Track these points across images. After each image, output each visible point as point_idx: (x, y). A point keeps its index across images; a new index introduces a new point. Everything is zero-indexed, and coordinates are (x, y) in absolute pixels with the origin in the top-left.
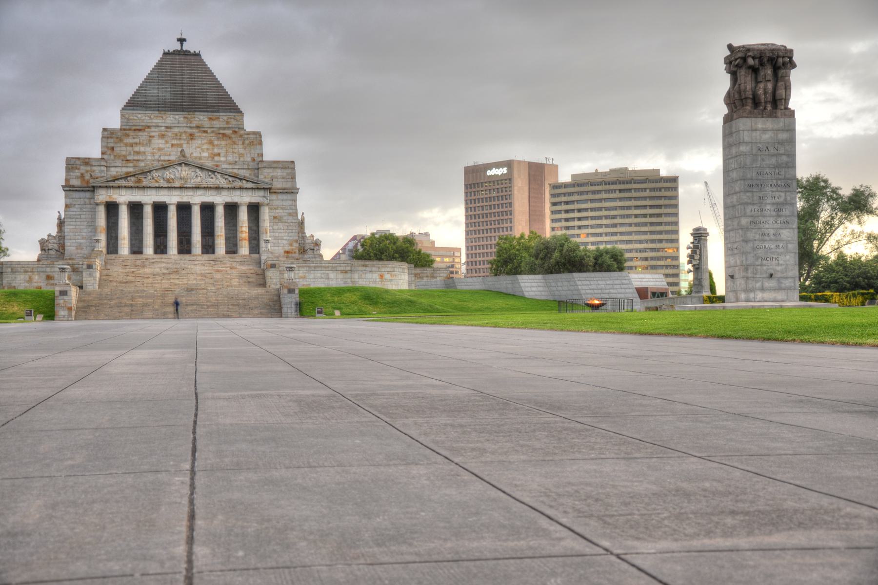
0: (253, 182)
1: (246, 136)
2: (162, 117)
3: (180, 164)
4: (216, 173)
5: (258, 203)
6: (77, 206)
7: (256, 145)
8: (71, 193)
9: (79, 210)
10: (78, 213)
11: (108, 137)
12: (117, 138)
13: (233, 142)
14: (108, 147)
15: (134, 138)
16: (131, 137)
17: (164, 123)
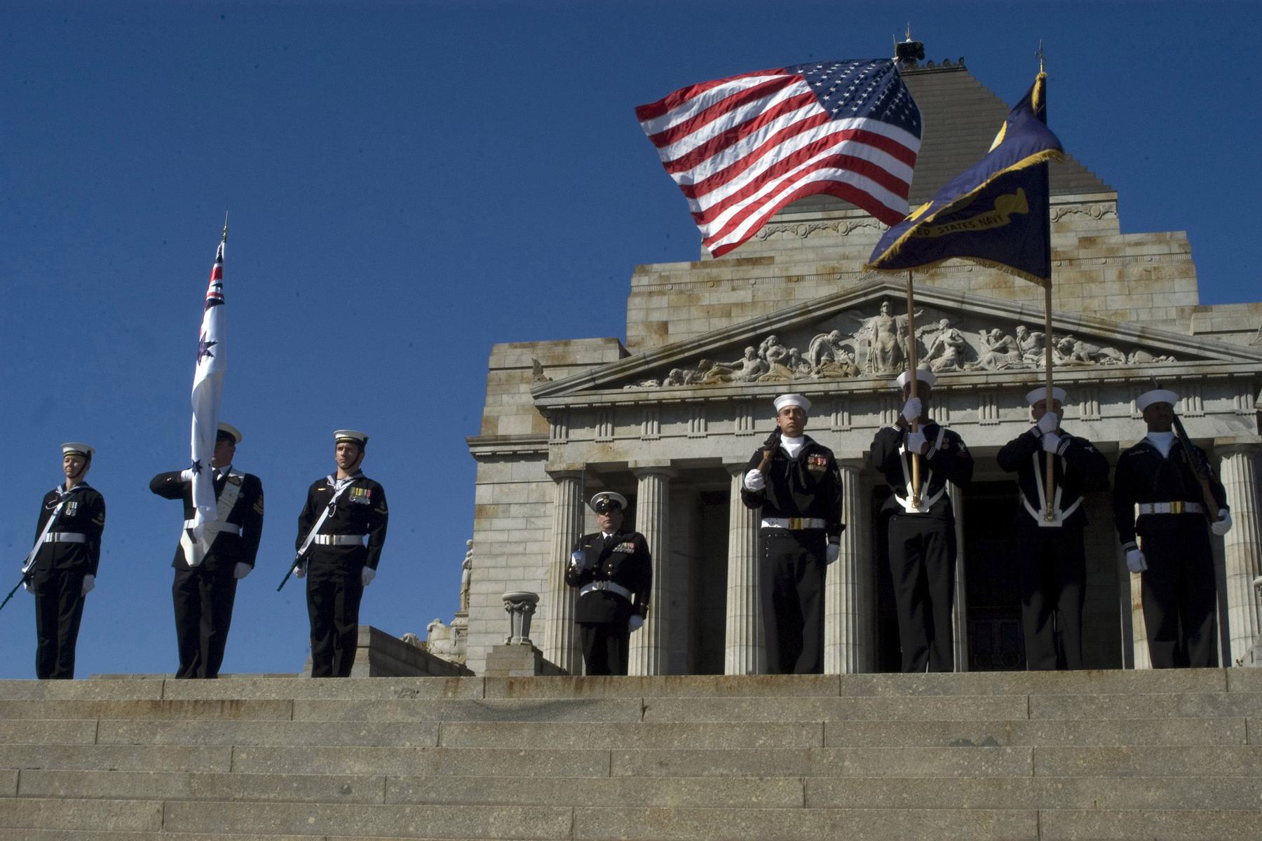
0: (1180, 356)
1: (1130, 251)
2: (836, 228)
3: (871, 308)
4: (1020, 330)
5: (1212, 440)
6: (514, 510)
7: (1172, 278)
8: (501, 465)
9: (521, 523)
10: (516, 536)
11: (651, 294)
12: (681, 292)
13: (1084, 273)
14: (648, 325)
15: (733, 289)
16: (726, 286)
17: (843, 245)
